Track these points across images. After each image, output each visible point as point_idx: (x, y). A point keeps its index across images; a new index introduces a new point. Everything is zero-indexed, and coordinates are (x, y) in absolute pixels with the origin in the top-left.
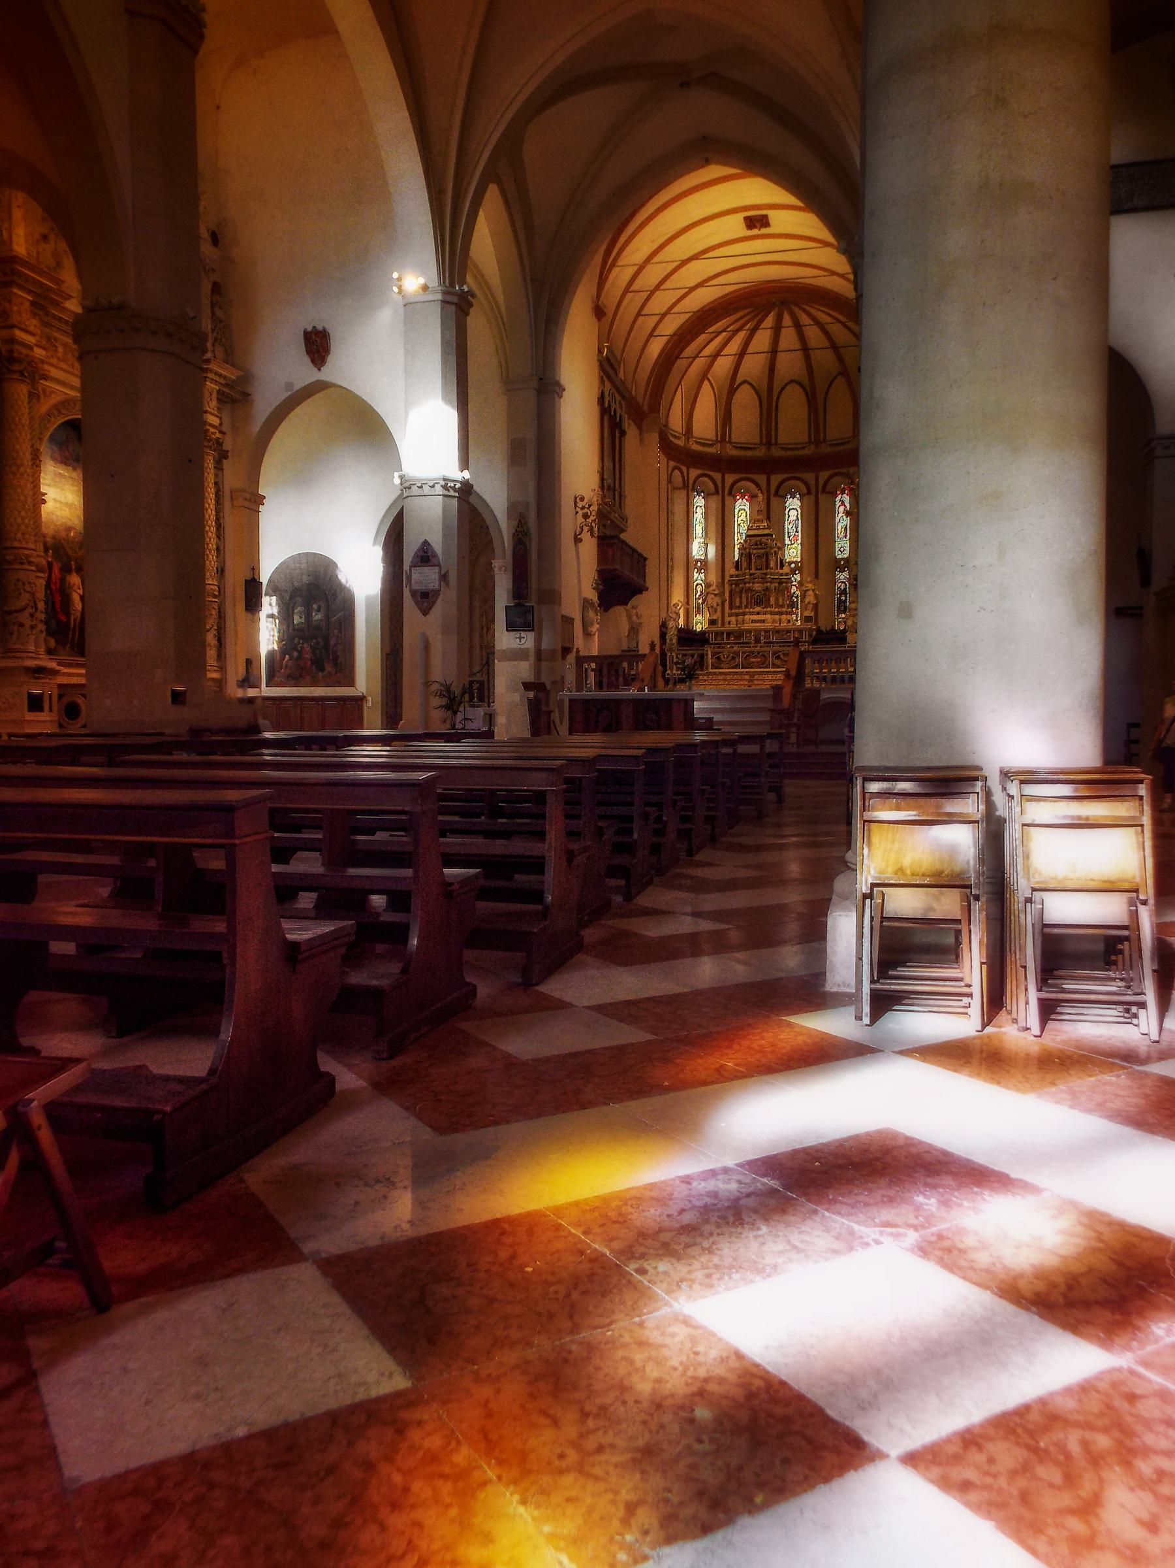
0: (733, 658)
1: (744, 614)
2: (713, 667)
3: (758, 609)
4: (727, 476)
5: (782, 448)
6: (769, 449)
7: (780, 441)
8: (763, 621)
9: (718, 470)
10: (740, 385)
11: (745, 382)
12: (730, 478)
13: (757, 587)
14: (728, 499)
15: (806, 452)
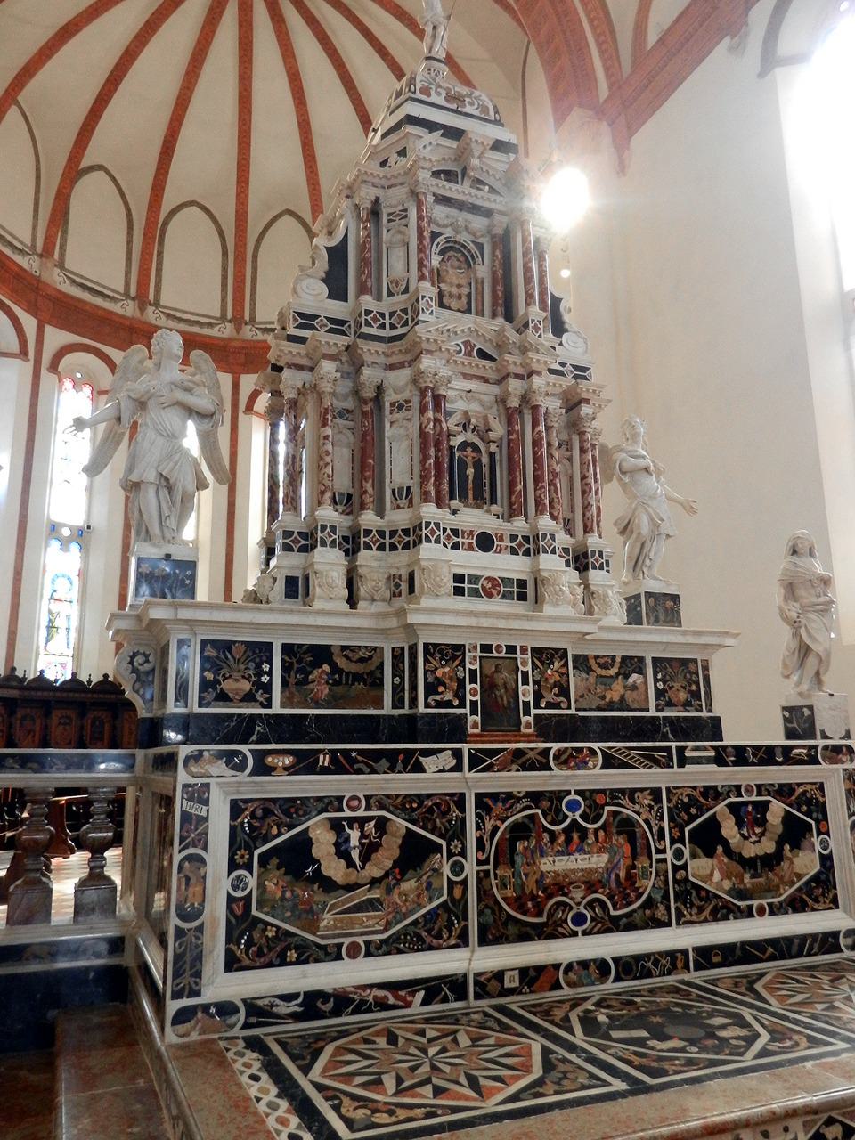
0: (414, 854)
1: (411, 537)
2: (252, 943)
3: (474, 519)
4: (49, 329)
5: (169, 316)
6: (142, 308)
7: (162, 303)
8: (523, 591)
9: (33, 310)
10: (91, 169)
11: (100, 167)
12: (56, 337)
13: (466, 398)
14: (47, 378)
15: (213, 332)
